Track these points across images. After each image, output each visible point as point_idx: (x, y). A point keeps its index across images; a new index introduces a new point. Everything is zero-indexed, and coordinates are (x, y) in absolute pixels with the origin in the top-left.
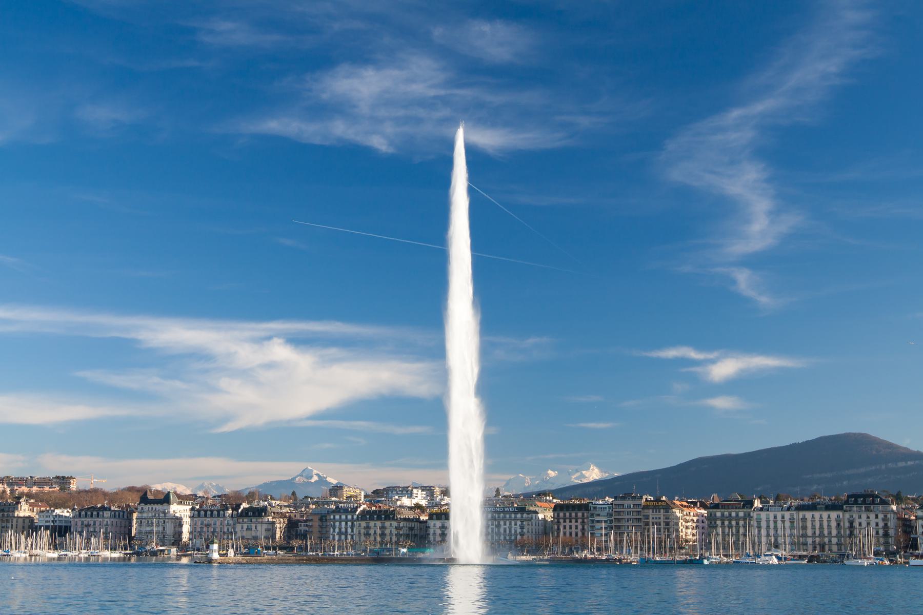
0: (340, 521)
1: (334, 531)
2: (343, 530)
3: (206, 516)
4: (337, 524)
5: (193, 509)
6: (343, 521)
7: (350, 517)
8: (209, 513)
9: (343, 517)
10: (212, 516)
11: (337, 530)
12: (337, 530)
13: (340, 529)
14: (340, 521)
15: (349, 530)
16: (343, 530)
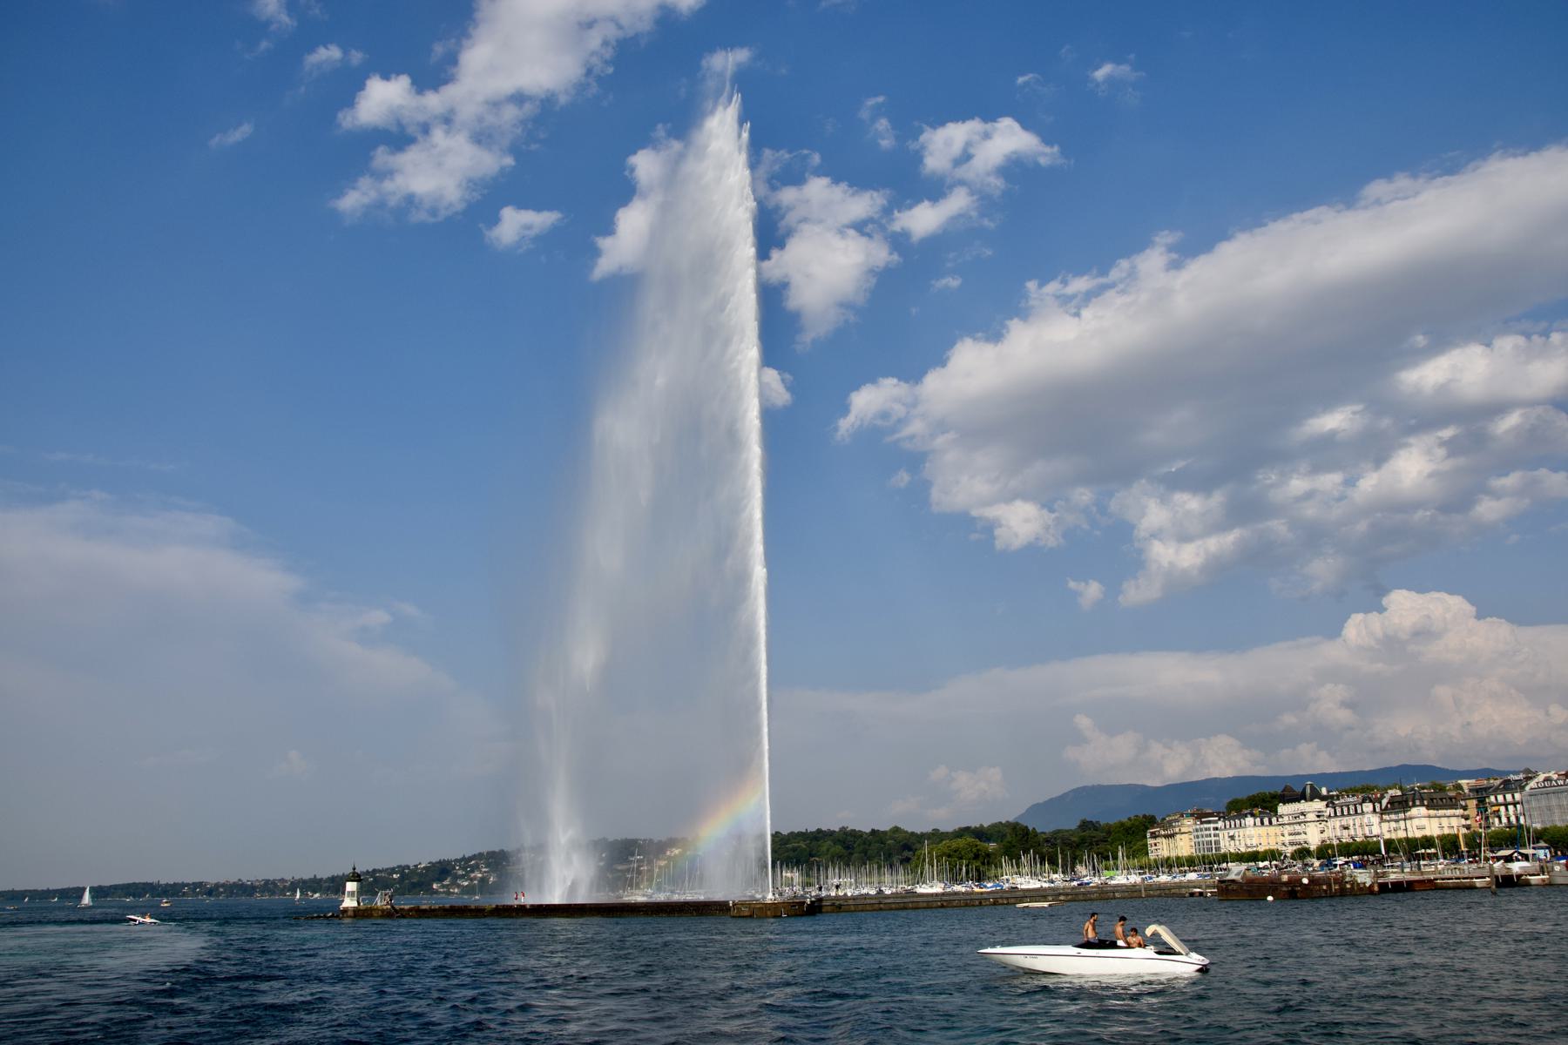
0: (1506, 805)
1: (1500, 822)
2: (1513, 819)
3: (1343, 815)
4: (1502, 809)
5: (1327, 806)
6: (1510, 804)
7: (1517, 796)
8: (1345, 809)
9: (1509, 797)
10: (1349, 814)
11: (1504, 820)
12: (1504, 820)
13: (1508, 818)
14: (1506, 805)
15: (1522, 821)
16: (1513, 819)
